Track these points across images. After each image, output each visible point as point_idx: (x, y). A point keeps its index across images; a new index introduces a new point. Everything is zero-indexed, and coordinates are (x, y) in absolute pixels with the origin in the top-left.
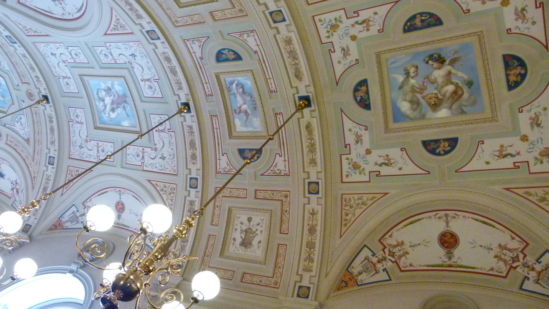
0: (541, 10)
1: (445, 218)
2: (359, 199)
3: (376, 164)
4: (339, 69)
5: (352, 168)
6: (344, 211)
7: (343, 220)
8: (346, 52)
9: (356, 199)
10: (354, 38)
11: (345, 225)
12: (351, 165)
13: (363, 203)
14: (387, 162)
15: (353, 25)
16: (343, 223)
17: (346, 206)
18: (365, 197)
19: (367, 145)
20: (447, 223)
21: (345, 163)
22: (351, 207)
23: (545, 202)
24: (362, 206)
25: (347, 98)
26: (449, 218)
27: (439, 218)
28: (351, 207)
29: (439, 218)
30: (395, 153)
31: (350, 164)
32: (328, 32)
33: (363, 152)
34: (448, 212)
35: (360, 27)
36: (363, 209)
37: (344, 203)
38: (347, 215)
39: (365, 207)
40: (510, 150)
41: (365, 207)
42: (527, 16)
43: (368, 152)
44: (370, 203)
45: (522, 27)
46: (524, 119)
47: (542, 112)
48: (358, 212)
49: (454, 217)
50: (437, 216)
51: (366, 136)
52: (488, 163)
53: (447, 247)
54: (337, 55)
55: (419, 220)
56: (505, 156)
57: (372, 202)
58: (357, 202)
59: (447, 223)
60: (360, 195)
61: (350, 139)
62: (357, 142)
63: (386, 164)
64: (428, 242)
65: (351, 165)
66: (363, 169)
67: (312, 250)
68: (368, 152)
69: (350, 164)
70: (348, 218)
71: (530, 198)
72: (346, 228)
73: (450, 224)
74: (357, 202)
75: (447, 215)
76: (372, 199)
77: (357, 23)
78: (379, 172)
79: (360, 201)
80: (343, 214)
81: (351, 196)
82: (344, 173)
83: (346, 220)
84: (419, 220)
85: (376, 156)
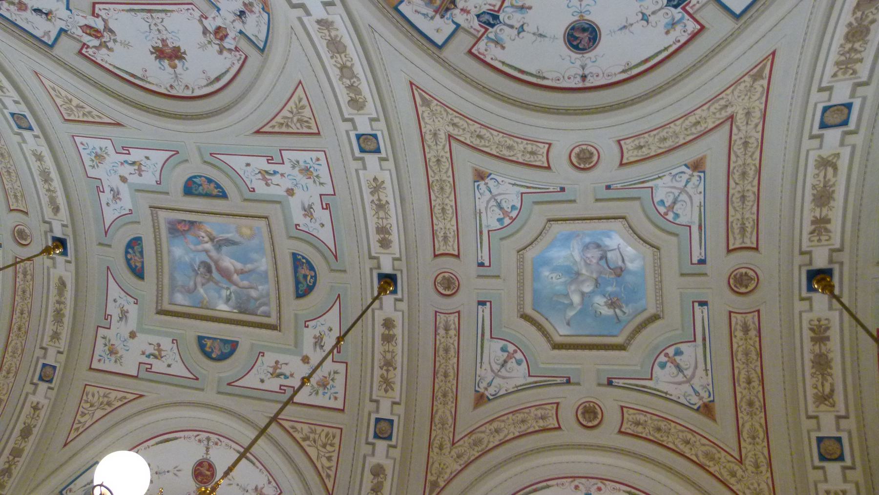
0: (328, 211)
1: (206, 443)
2: (105, 396)
3: (143, 353)
4: (110, 215)
5: (108, 352)
6: (81, 409)
7: (76, 422)
8: (116, 195)
9: (102, 394)
10: (124, 179)
11: (78, 429)
12: (107, 348)
13: (109, 404)
14: (156, 353)
15: (122, 164)
16: (75, 426)
17: (87, 402)
18: (113, 395)
19: (133, 323)
20: (208, 449)
21: (100, 342)
22: (92, 406)
23: (308, 442)
24: (106, 407)
25: (116, 256)
26: (211, 444)
27: (200, 441)
29: (200, 441)
30: (166, 343)
31: (106, 345)
32: (93, 161)
34: (211, 435)
35: (132, 169)
36: (107, 411)
37: (85, 398)
38: (83, 414)
39: (109, 409)
40: (285, 370)
42: (315, 215)
43: (133, 335)
45: (312, 227)
46: (308, 335)
47: (327, 332)
48: (99, 414)
49: (217, 444)
50: (197, 438)
51: (133, 310)
52: (262, 381)
53: (201, 482)
54: (106, 197)
55: (176, 439)
56: (278, 376)
57: (120, 403)
58: (101, 399)
59: (208, 449)
60: (109, 391)
61: (113, 310)
62: (121, 319)
63: (156, 357)
64: (179, 471)
65: (107, 348)
66: (121, 357)
67: (16, 459)
68: (133, 335)
69: (106, 345)
70: (83, 420)
71: (295, 434)
72: (76, 434)
73: (211, 451)
74: (101, 399)
75: (208, 439)
76: (120, 400)
77: (126, 162)
79: (106, 400)
80: (80, 412)
82: (96, 357)
83: (80, 422)
84: (176, 439)
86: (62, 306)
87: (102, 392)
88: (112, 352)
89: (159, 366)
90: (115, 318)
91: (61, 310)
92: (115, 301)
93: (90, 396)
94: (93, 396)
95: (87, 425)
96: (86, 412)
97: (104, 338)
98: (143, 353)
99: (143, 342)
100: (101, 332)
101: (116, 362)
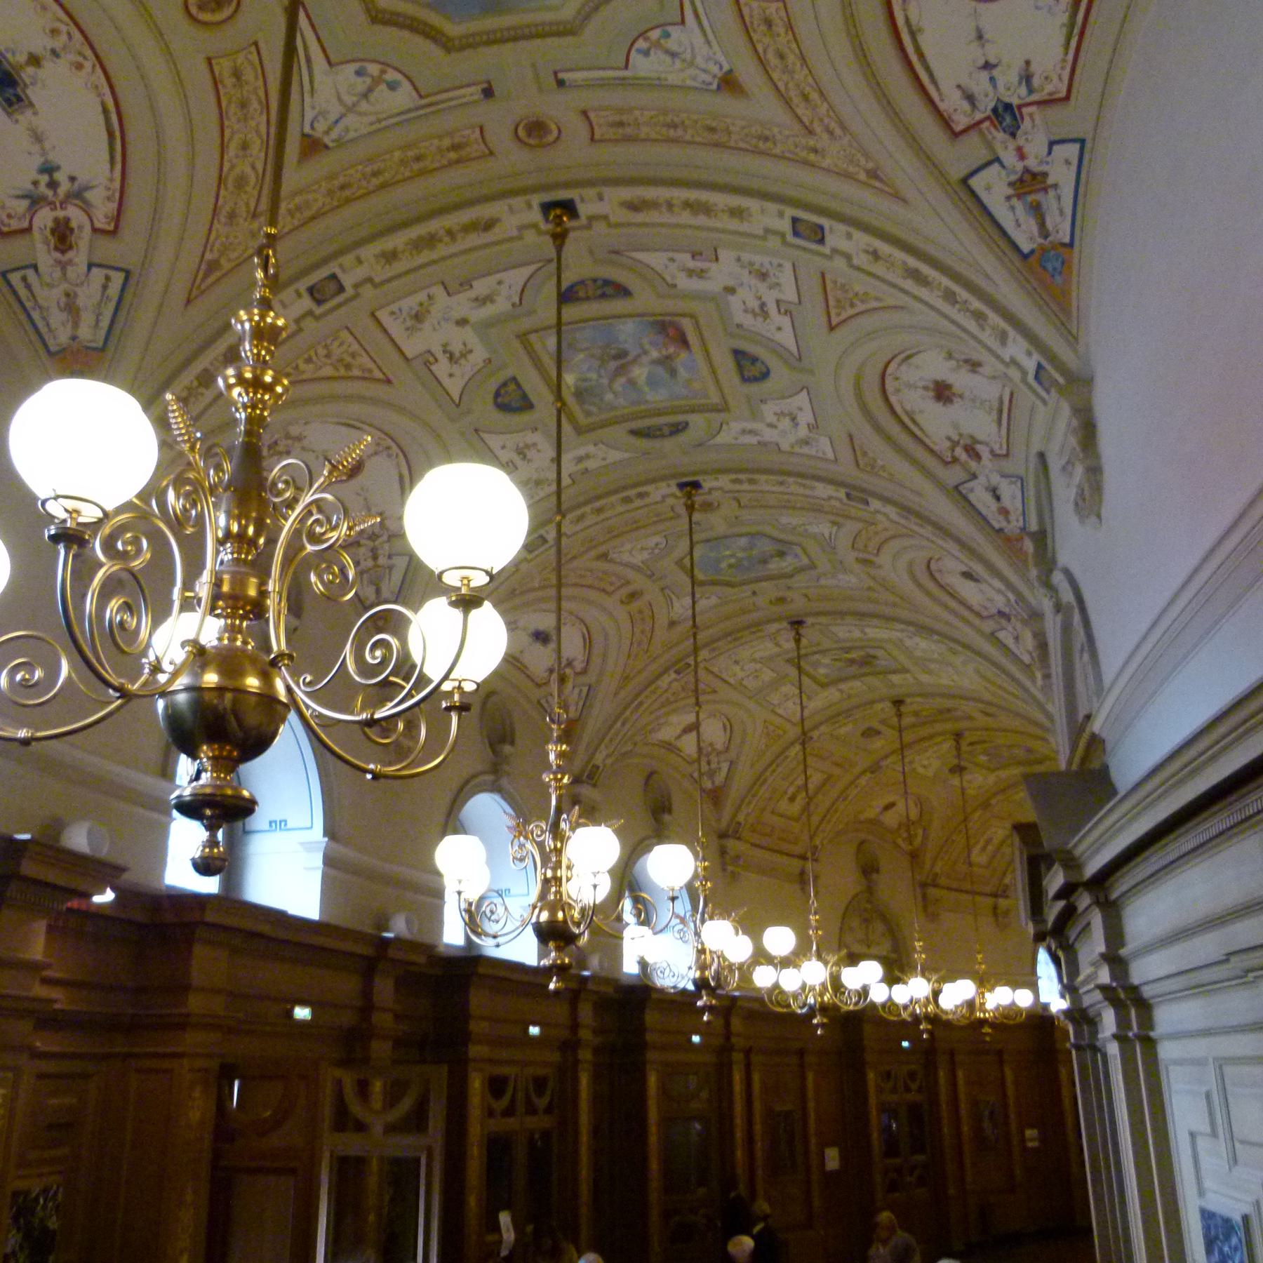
2: (353, 355)
5: (414, 312)
9: (351, 350)
13: (348, 367)
17: (326, 346)
18: (365, 360)
21: (421, 296)
28: (328, 356)
33: (456, 315)
38: (309, 360)
39: (342, 372)
41: (342, 372)
44: (356, 372)
48: (328, 371)
61: (481, 287)
62: (476, 299)
66: (420, 329)
70: (302, 366)
78: (436, 360)
81: (351, 339)
83: (297, 367)
85: (459, 338)
86: (447, 239)
87: (356, 347)
88: (418, 317)
89: (442, 368)
90: (472, 294)
91: (441, 241)
92: (500, 283)
93: (336, 344)
94: (342, 344)
95: (304, 377)
96: (314, 358)
97: (430, 297)
98: (445, 346)
99: (459, 338)
100: (438, 291)
101: (407, 329)
